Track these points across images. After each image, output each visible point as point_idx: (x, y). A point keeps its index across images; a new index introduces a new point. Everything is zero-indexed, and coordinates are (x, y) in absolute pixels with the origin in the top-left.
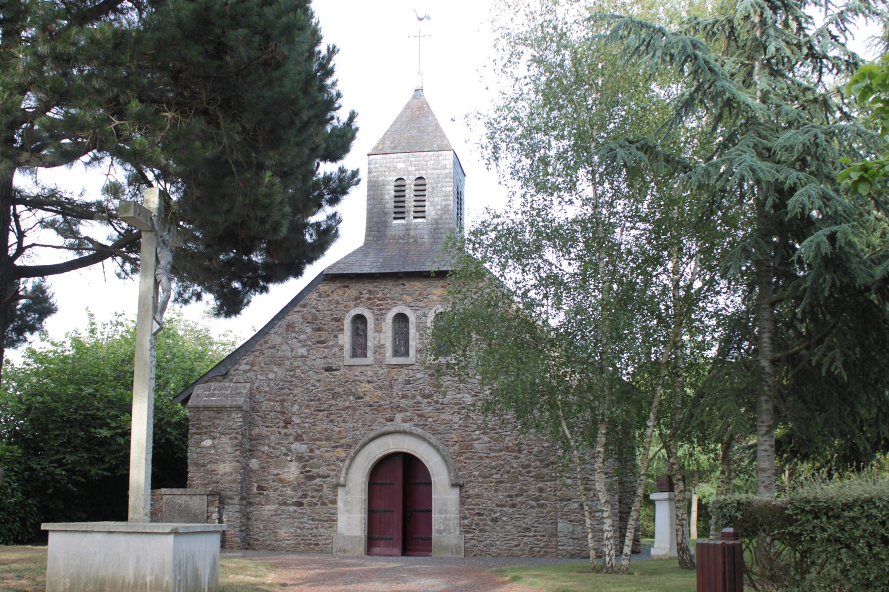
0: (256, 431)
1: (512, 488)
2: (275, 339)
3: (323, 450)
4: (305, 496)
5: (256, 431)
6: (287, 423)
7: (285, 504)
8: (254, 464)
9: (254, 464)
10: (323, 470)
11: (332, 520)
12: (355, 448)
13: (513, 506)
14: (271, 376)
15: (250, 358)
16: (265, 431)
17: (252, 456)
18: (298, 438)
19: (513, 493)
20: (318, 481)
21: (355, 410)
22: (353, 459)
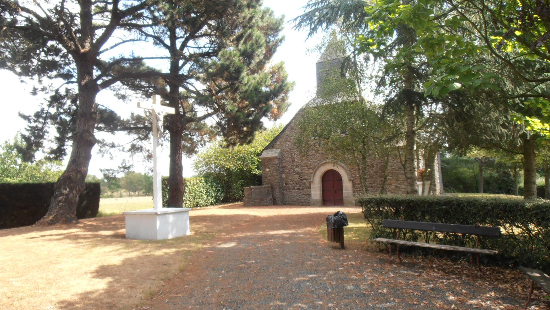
0: (283, 165)
1: (371, 181)
2: (287, 133)
3: (306, 171)
4: (300, 186)
5: (283, 165)
6: (293, 161)
7: (294, 189)
8: (284, 176)
9: (284, 176)
10: (306, 177)
11: (310, 194)
12: (315, 169)
13: (372, 187)
14: (287, 146)
15: (280, 140)
16: (286, 164)
17: (283, 173)
18: (297, 166)
19: (371, 182)
20: (304, 181)
21: (315, 155)
22: (315, 173)
